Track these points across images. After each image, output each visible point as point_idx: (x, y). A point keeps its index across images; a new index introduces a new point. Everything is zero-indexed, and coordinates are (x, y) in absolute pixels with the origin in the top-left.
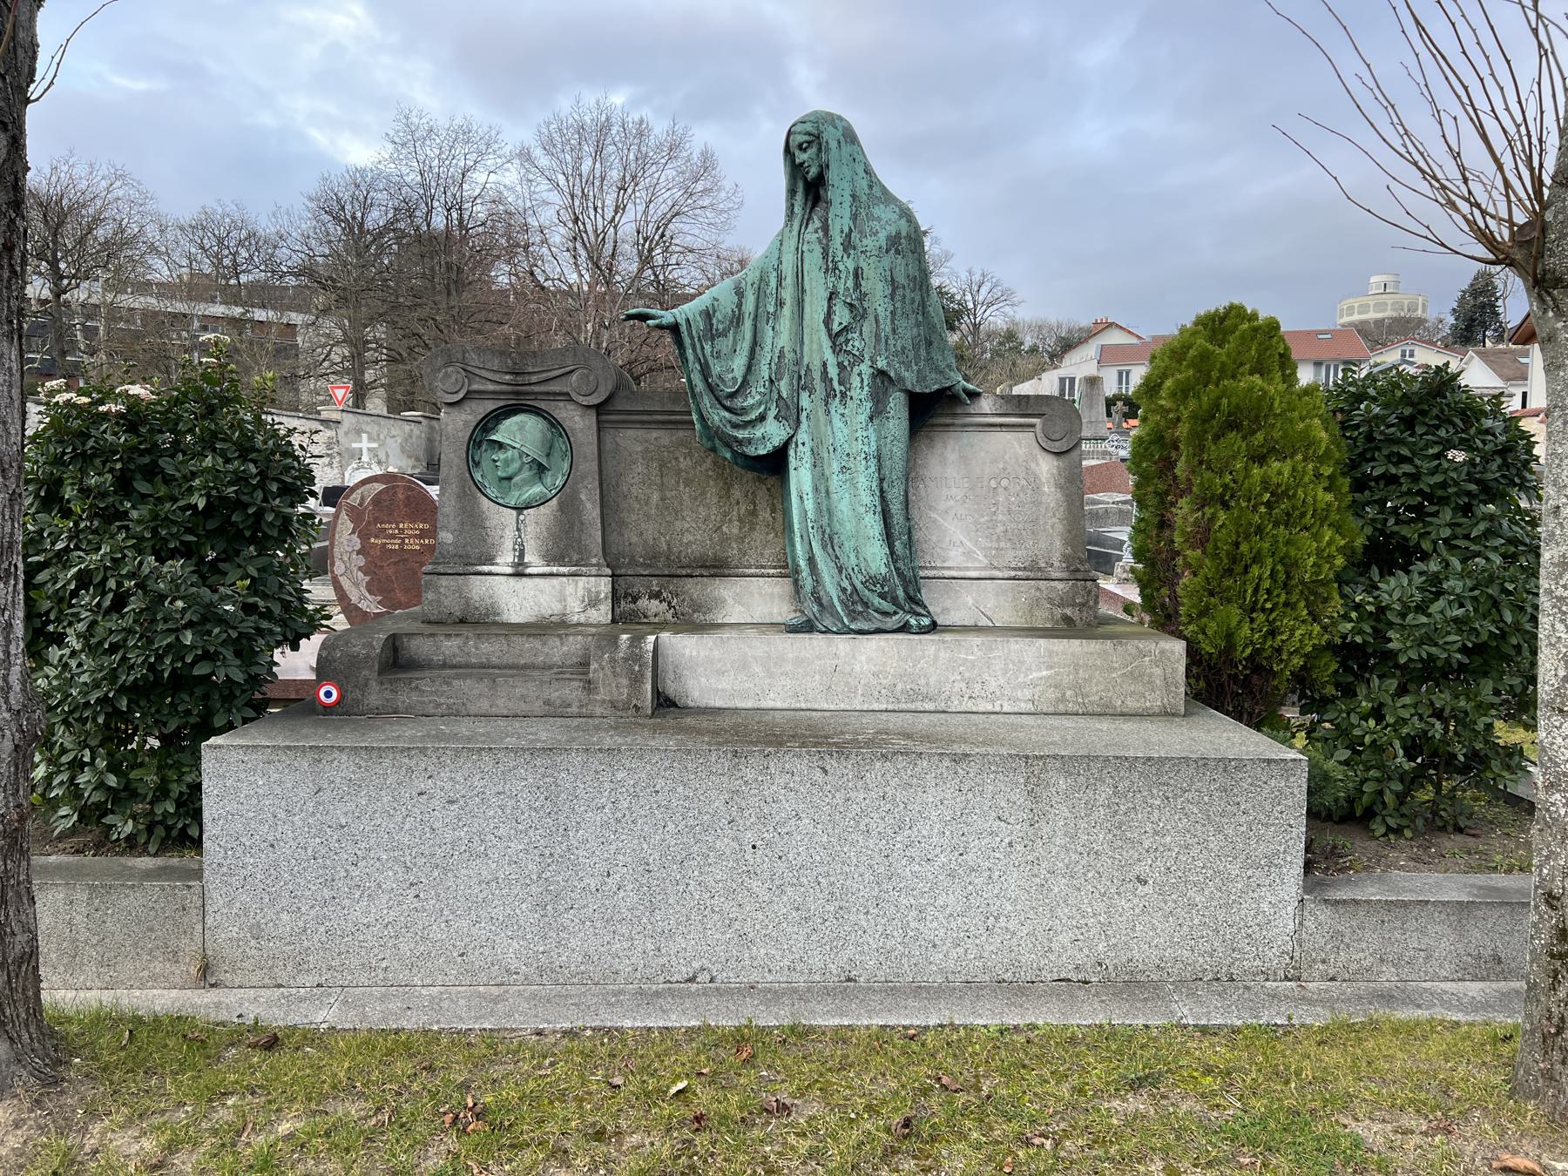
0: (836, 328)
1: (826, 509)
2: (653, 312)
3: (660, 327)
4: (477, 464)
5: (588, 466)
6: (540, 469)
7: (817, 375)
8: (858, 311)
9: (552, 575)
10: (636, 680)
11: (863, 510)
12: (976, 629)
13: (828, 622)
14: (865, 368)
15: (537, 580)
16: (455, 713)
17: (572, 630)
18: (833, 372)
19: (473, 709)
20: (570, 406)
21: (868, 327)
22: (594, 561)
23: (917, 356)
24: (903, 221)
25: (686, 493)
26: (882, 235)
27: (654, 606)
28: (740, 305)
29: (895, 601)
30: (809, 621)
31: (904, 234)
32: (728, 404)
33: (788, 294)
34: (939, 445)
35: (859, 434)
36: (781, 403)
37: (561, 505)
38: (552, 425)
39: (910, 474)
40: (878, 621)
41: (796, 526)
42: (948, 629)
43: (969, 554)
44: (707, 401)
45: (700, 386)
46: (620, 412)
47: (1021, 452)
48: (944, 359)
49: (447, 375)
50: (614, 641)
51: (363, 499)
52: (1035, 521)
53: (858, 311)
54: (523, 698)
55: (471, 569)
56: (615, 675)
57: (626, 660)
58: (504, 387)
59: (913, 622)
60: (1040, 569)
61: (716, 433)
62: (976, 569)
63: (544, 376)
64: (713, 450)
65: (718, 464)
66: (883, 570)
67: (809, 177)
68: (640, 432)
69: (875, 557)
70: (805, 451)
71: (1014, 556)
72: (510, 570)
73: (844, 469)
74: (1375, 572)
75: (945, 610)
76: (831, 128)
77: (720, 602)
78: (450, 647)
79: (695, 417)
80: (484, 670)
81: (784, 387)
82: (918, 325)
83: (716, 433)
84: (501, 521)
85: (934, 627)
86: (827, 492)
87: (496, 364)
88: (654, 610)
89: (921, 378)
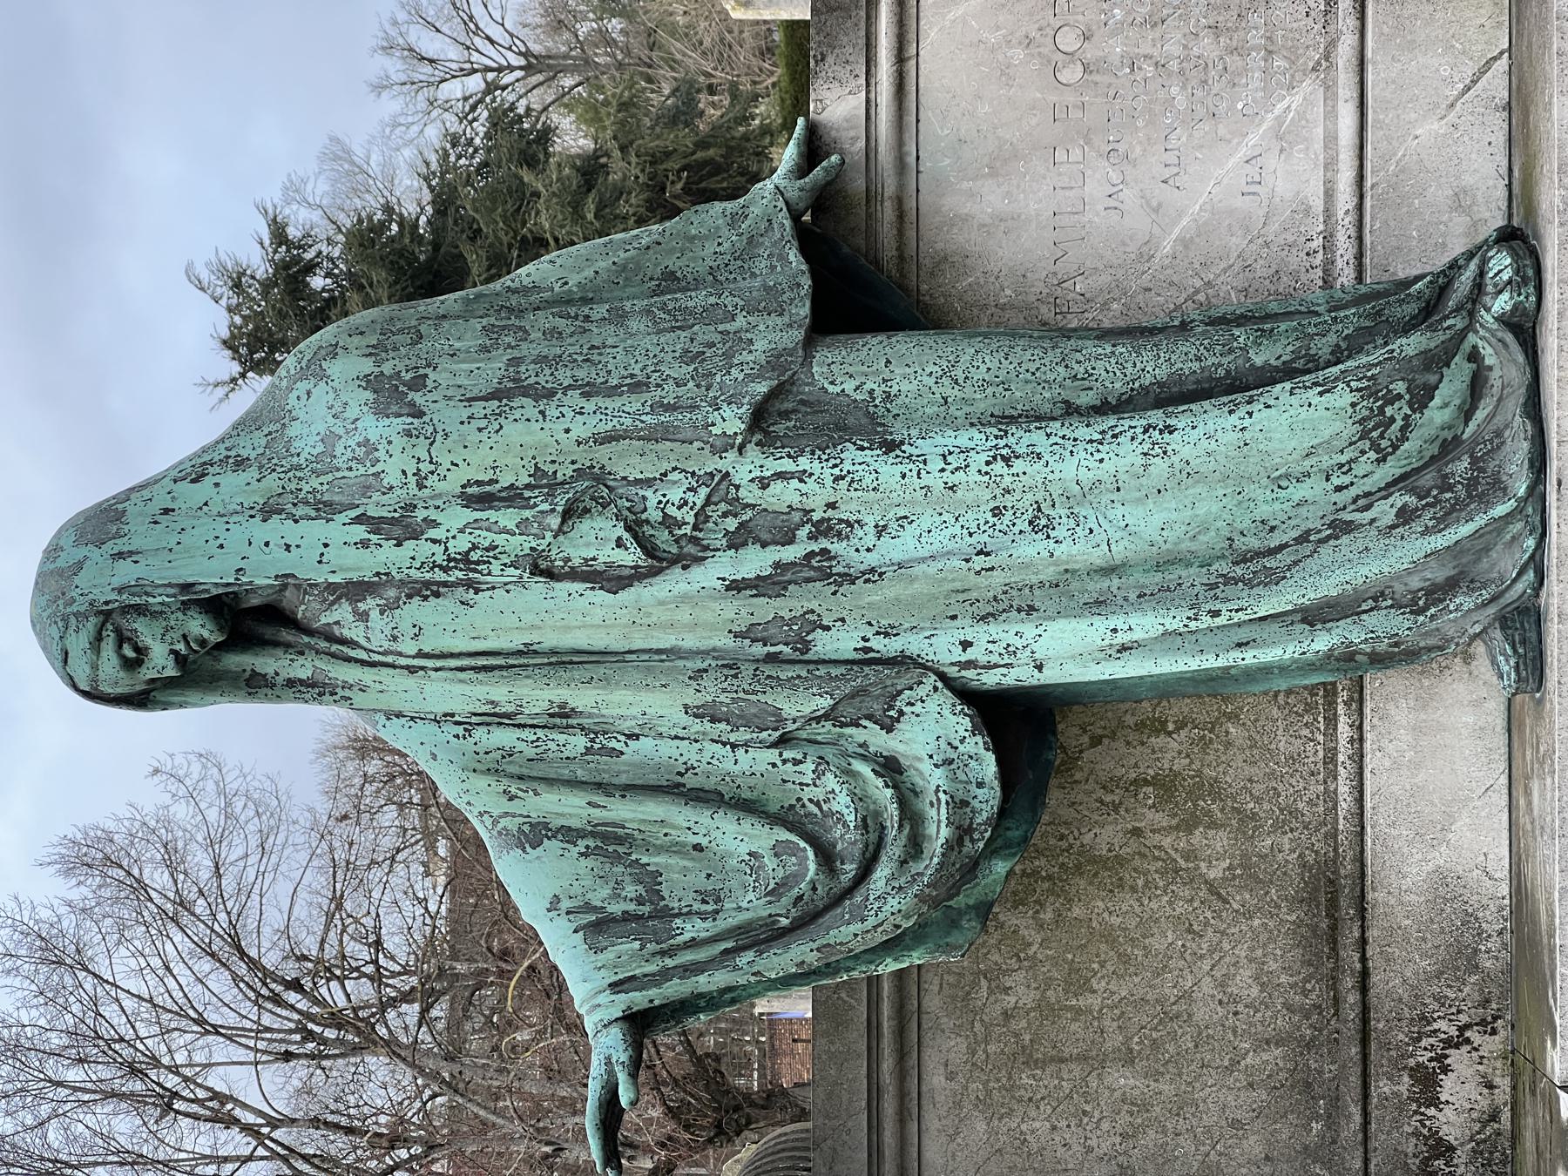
0: (631, 557)
1: (1159, 577)
2: (594, 1091)
7: (765, 609)
8: (585, 493)
11: (1159, 466)
12: (1520, 109)
13: (1507, 562)
14: (745, 468)
18: (755, 562)
21: (628, 463)
23: (709, 315)
24: (335, 368)
25: (1106, 989)
26: (373, 428)
27: (1462, 1094)
28: (569, 834)
29: (1436, 361)
30: (1504, 621)
31: (367, 366)
32: (850, 869)
33: (537, 695)
34: (959, 239)
35: (935, 481)
36: (848, 711)
39: (1047, 323)
40: (1502, 408)
41: (1211, 662)
42: (1521, 189)
43: (1284, 138)
44: (845, 932)
45: (801, 952)
48: (714, 234)
53: (585, 493)
59: (1502, 303)
61: (935, 903)
62: (1331, 114)
64: (984, 911)
65: (1020, 894)
66: (1342, 398)
67: (215, 638)
68: (932, 1122)
69: (1303, 423)
70: (987, 640)
73: (1040, 524)
75: (1461, 201)
76: (82, 580)
79: (889, 966)
81: (798, 705)
82: (618, 317)
83: (935, 903)
85: (1518, 238)
86: (1109, 571)
88: (1473, 1091)
89: (770, 303)
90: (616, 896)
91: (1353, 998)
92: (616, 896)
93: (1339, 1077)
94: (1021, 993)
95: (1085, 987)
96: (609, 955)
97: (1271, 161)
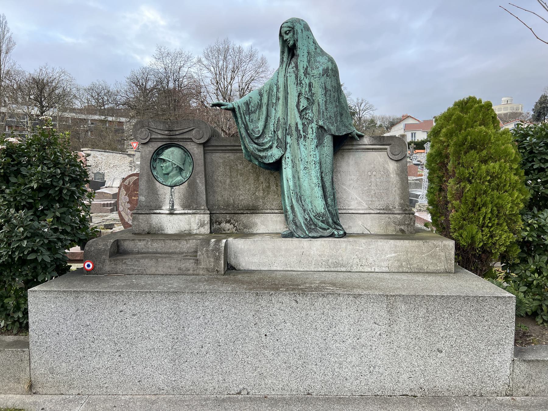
0: (301, 108)
1: (298, 185)
3: (226, 109)
4: (155, 168)
5: (200, 168)
6: (180, 170)
7: (293, 128)
8: (311, 101)
9: (185, 214)
10: (217, 259)
11: (313, 185)
12: (363, 235)
13: (299, 233)
14: (314, 125)
15: (179, 216)
16: (141, 274)
17: (192, 237)
18: (300, 127)
19: (148, 272)
20: (192, 144)
21: (315, 108)
22: (203, 208)
23: (336, 120)
24: (330, 63)
25: (241, 179)
26: (321, 69)
27: (228, 226)
28: (261, 100)
29: (328, 224)
30: (291, 232)
31: (330, 68)
32: (256, 141)
33: (281, 95)
34: (346, 158)
35: (312, 153)
36: (279, 141)
37: (189, 185)
38: (185, 152)
39: (334, 170)
40: (321, 232)
41: (286, 193)
42: (351, 235)
43: (359, 203)
44: (247, 140)
46: (213, 146)
47: (381, 160)
48: (348, 121)
49: (142, 132)
50: (208, 242)
51: (129, 182)
52: (387, 189)
53: (311, 101)
54: (170, 267)
55: (152, 212)
56: (208, 257)
57: (213, 250)
58: (165, 137)
59: (336, 233)
60: (390, 209)
61: (251, 154)
62: (362, 210)
63: (181, 131)
64: (250, 161)
66: (323, 211)
67: (289, 45)
68: (222, 155)
69: (319, 205)
70: (289, 161)
71: (379, 204)
72: (168, 212)
73: (305, 168)
74: (535, 210)
75: (350, 227)
76: (298, 24)
77: (255, 224)
78: (140, 245)
79: (242, 147)
80: (155, 255)
81: (280, 134)
82: (336, 107)
83: (251, 154)
84: (165, 191)
85: (345, 235)
86: (299, 178)
87: (161, 127)
88: (228, 228)
89: (338, 129)
90: (252, 107)
91: (240, 212)
92: (252, 107)
93: (229, 210)
94: (240, 167)
95: (241, 176)
96: (243, 105)
97: (356, 201)
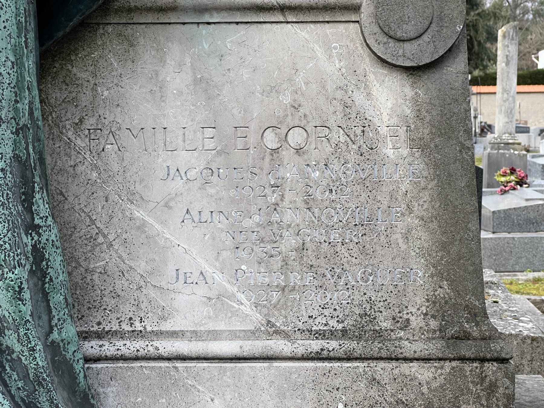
34: (146, 56)
43: (219, 301)
47: (332, 67)
52: (366, 225)
60: (378, 334)
62: (234, 335)
71: (319, 305)
97: (201, 291)
